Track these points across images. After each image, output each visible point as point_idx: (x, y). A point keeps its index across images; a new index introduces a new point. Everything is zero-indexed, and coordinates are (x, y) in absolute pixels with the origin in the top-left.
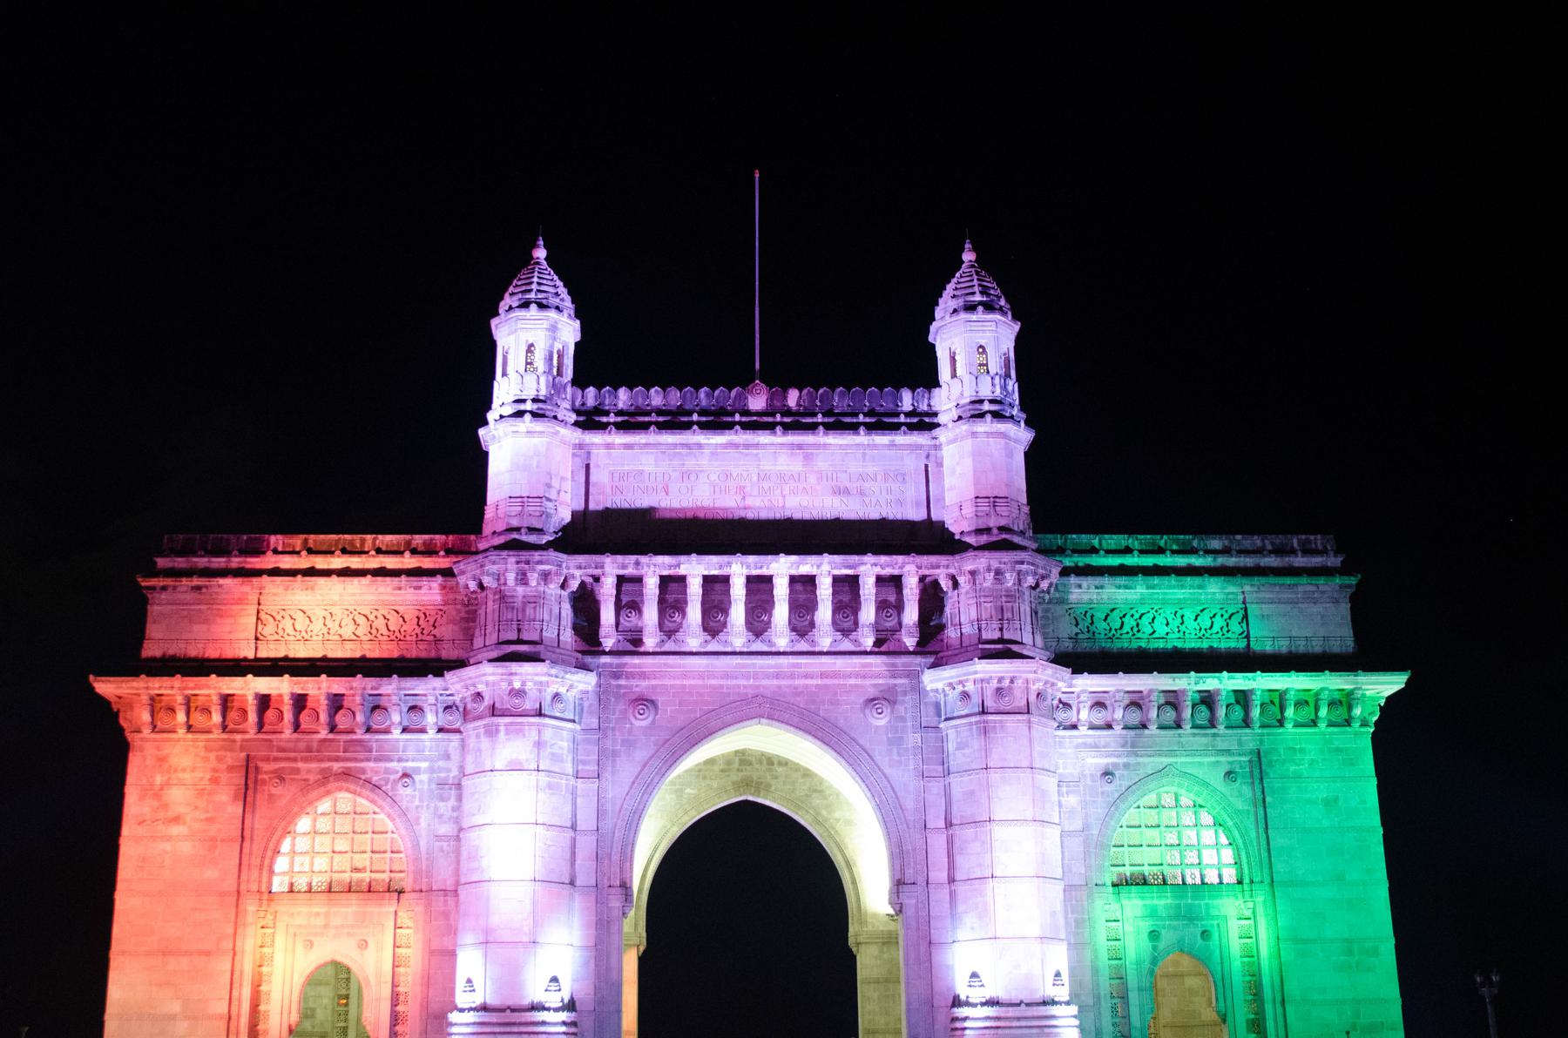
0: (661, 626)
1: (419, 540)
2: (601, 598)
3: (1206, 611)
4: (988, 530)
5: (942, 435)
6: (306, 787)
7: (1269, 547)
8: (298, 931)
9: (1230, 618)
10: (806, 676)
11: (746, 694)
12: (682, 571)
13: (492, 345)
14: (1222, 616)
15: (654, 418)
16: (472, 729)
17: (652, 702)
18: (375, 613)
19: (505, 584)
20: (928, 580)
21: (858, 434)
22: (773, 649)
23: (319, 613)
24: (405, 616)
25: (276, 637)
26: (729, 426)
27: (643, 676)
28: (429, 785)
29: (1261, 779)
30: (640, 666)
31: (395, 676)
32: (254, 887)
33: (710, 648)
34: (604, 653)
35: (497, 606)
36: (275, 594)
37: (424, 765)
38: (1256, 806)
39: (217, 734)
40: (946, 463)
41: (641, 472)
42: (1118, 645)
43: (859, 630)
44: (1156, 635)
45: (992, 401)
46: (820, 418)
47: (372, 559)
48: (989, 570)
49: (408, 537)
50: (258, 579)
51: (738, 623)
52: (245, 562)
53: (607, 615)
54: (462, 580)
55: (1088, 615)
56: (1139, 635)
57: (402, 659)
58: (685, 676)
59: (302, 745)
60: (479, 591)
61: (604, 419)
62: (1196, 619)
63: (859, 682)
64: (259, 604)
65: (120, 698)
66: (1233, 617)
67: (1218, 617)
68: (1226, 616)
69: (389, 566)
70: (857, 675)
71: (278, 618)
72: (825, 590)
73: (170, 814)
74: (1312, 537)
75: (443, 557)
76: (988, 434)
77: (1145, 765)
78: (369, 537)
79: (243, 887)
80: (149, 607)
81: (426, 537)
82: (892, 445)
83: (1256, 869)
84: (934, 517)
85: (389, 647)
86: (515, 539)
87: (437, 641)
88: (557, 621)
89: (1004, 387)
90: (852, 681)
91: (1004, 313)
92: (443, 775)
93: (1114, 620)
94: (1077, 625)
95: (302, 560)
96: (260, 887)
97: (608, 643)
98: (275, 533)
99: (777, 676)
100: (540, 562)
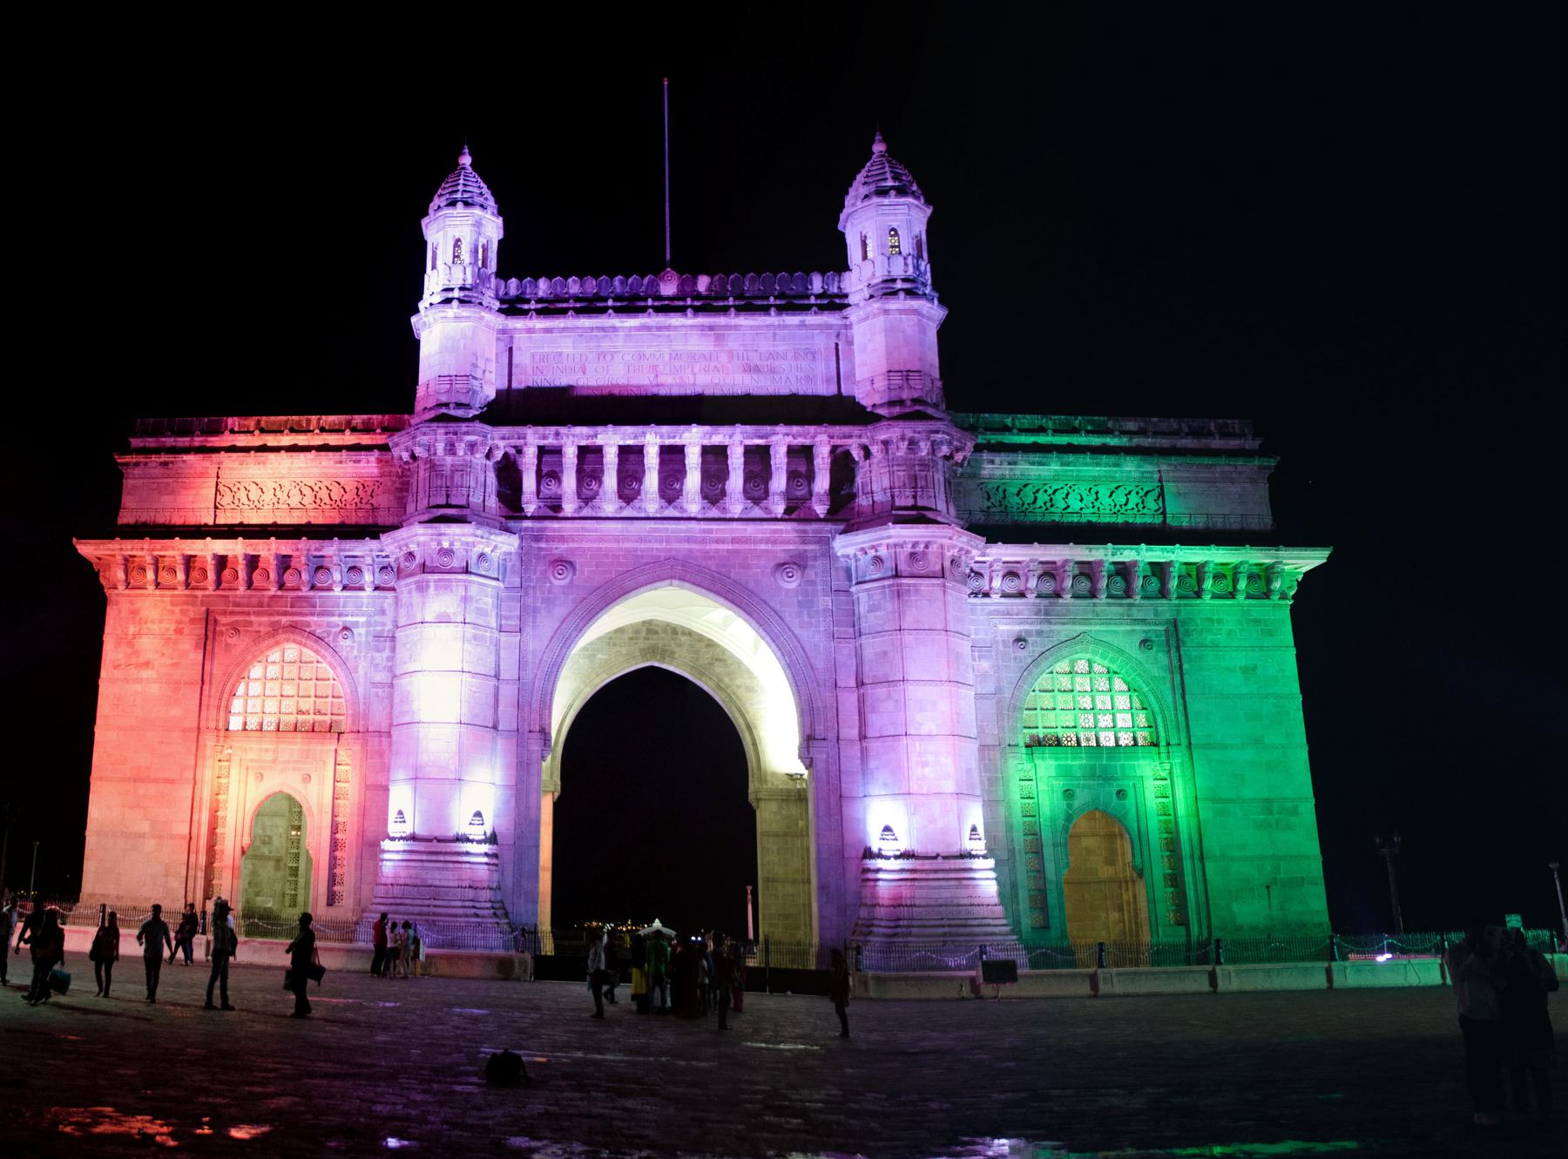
0: (579, 493)
2: (523, 468)
3: (1122, 488)
6: (258, 638)
7: (1186, 429)
8: (250, 764)
9: (1146, 495)
10: (718, 541)
11: (659, 557)
12: (599, 441)
14: (1137, 493)
16: (406, 586)
17: (571, 563)
18: (319, 484)
19: (435, 454)
20: (839, 450)
21: (769, 315)
22: (685, 515)
23: (269, 485)
24: (346, 488)
25: (232, 506)
27: (562, 539)
28: (366, 637)
30: (559, 530)
31: (336, 539)
32: (212, 725)
33: (627, 513)
34: (526, 518)
35: (427, 474)
36: (230, 469)
37: (362, 619)
39: (181, 591)
40: (857, 340)
42: (1030, 518)
43: (770, 498)
44: (1069, 510)
45: (904, 280)
47: (317, 437)
48: (903, 439)
49: (348, 417)
50: (217, 455)
51: (652, 490)
52: (206, 441)
53: (529, 482)
54: (396, 452)
55: (1001, 490)
56: (1053, 510)
57: (342, 525)
58: (600, 539)
59: (255, 601)
60: (411, 461)
62: (1110, 496)
63: (770, 547)
64: (218, 477)
65: (100, 559)
66: (1149, 495)
67: (1134, 493)
68: (1142, 493)
69: (332, 443)
70: (768, 541)
71: (235, 489)
72: (736, 460)
73: (141, 660)
74: (1229, 421)
75: (380, 434)
76: (901, 311)
77: (1059, 632)
78: (314, 418)
79: (203, 724)
80: (124, 481)
81: (365, 417)
84: (844, 392)
85: (332, 514)
86: (444, 414)
87: (374, 509)
88: (483, 488)
90: (763, 547)
91: (917, 198)
92: (379, 628)
93: (1026, 495)
95: (255, 438)
96: (217, 725)
97: (530, 508)
98: (233, 415)
99: (688, 540)
100: (467, 433)
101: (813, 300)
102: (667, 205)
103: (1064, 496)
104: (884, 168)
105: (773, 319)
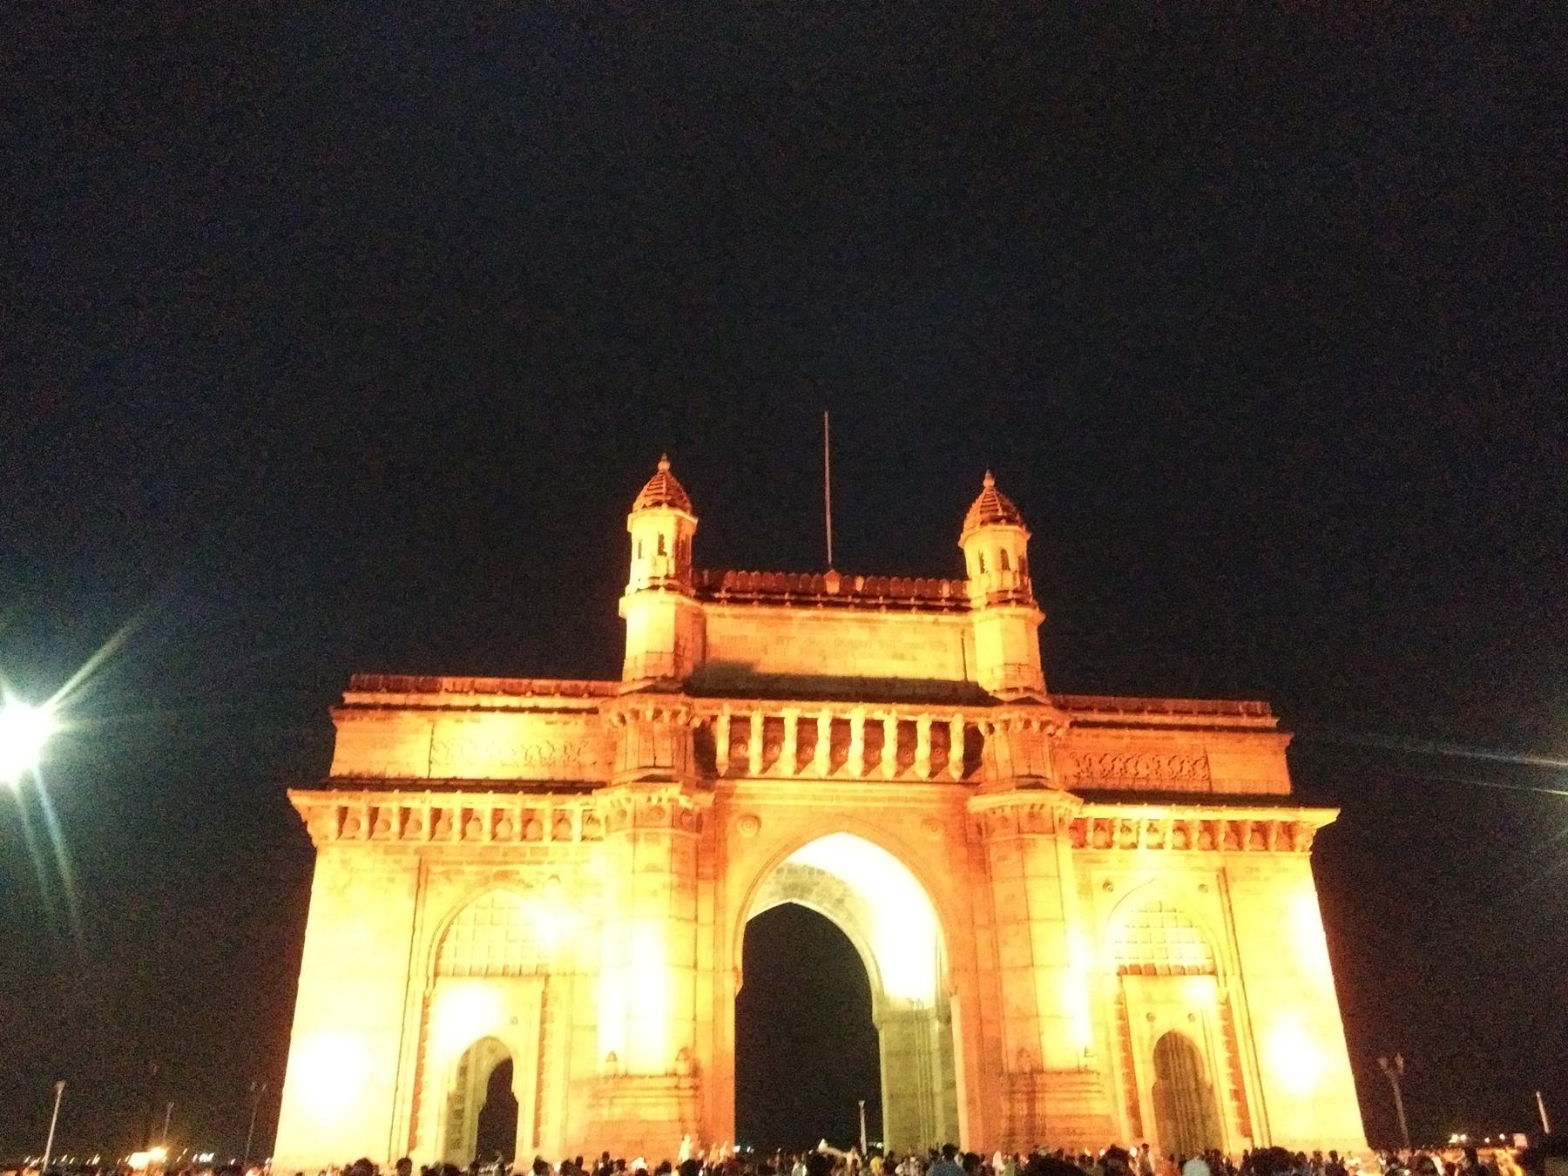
1: (566, 684)
4: (1016, 690)
5: (974, 617)
9: (1195, 763)
12: (782, 714)
13: (627, 537)
14: (1189, 762)
15: (755, 595)
26: (813, 604)
29: (1227, 891)
30: (747, 788)
34: (718, 777)
38: (1224, 913)
41: (746, 636)
46: (881, 600)
49: (559, 682)
53: (722, 746)
55: (1087, 758)
61: (717, 595)
62: (1169, 764)
63: (917, 805)
67: (1186, 762)
68: (1192, 763)
70: (915, 800)
74: (1252, 703)
82: (936, 622)
83: (1228, 962)
87: (581, 766)
89: (1022, 581)
91: (1021, 526)
94: (1079, 765)
97: (722, 770)
99: (856, 799)
101: (943, 603)
102: (828, 517)
103: (1134, 764)
104: (995, 500)
105: (913, 616)
